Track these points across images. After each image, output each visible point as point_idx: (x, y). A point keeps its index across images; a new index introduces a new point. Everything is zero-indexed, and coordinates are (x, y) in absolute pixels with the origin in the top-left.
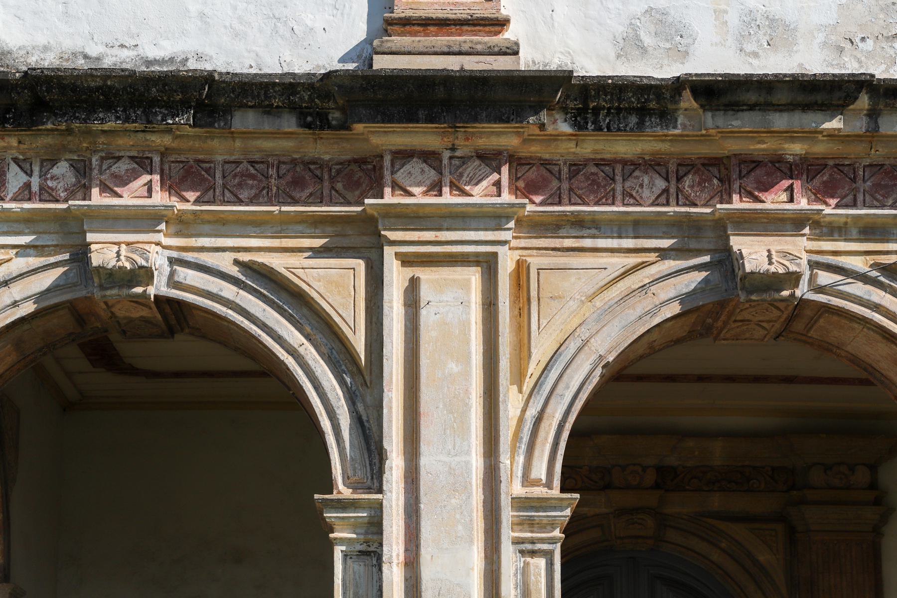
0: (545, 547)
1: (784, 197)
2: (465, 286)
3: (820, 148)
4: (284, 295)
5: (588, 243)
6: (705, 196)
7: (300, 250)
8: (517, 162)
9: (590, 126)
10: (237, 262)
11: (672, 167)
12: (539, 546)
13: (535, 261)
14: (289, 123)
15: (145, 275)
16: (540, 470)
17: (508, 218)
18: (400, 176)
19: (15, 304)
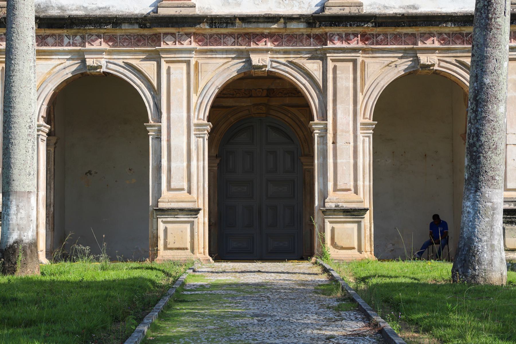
0: (202, 136)
1: (264, 44)
2: (182, 69)
3: (273, 31)
4: (136, 71)
5: (214, 56)
6: (244, 43)
7: (140, 59)
8: (195, 34)
9: (214, 27)
10: (123, 62)
11: (236, 35)
12: (201, 135)
13: (200, 61)
14: (136, 26)
15: (100, 67)
16: (201, 116)
17: (193, 51)
18: (165, 40)
19: (67, 74)
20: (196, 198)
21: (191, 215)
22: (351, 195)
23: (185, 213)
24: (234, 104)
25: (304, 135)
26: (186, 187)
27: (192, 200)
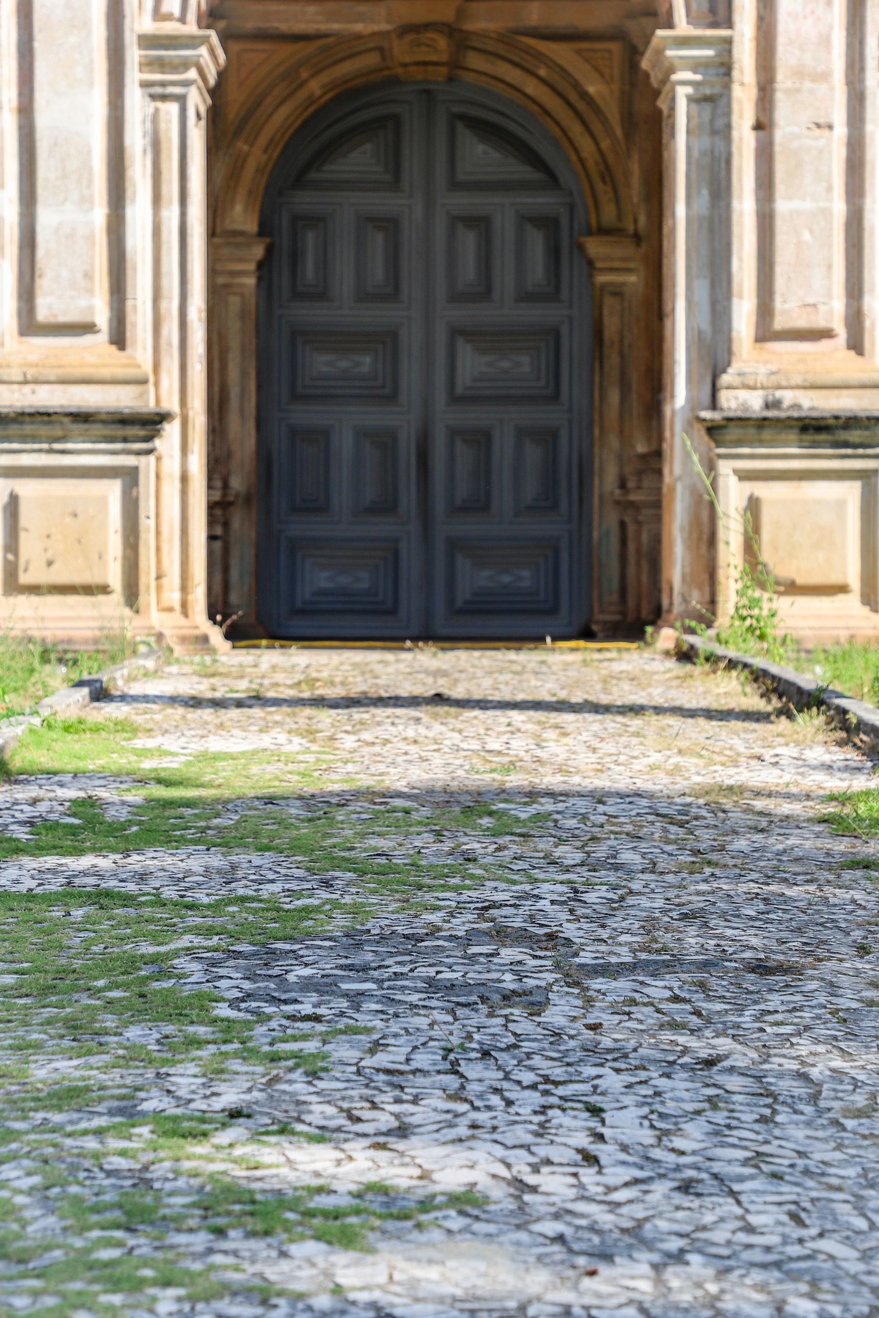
20: (147, 367)
21: (125, 440)
22: (832, 358)
23: (97, 429)
24: (324, 27)
25: (600, 151)
26: (102, 318)
27: (131, 373)
